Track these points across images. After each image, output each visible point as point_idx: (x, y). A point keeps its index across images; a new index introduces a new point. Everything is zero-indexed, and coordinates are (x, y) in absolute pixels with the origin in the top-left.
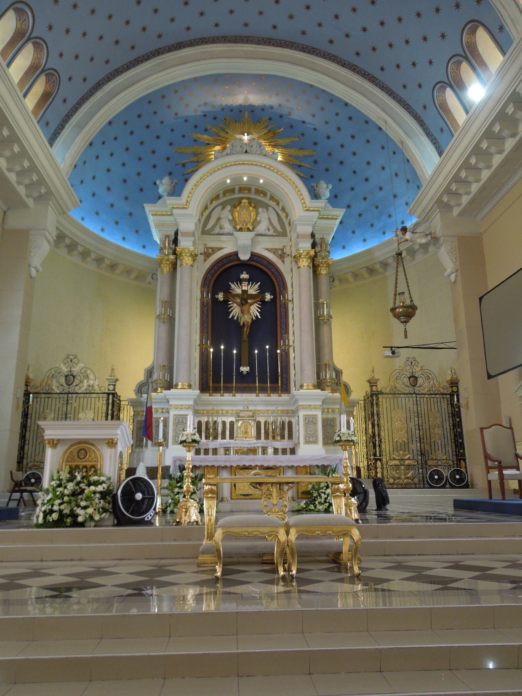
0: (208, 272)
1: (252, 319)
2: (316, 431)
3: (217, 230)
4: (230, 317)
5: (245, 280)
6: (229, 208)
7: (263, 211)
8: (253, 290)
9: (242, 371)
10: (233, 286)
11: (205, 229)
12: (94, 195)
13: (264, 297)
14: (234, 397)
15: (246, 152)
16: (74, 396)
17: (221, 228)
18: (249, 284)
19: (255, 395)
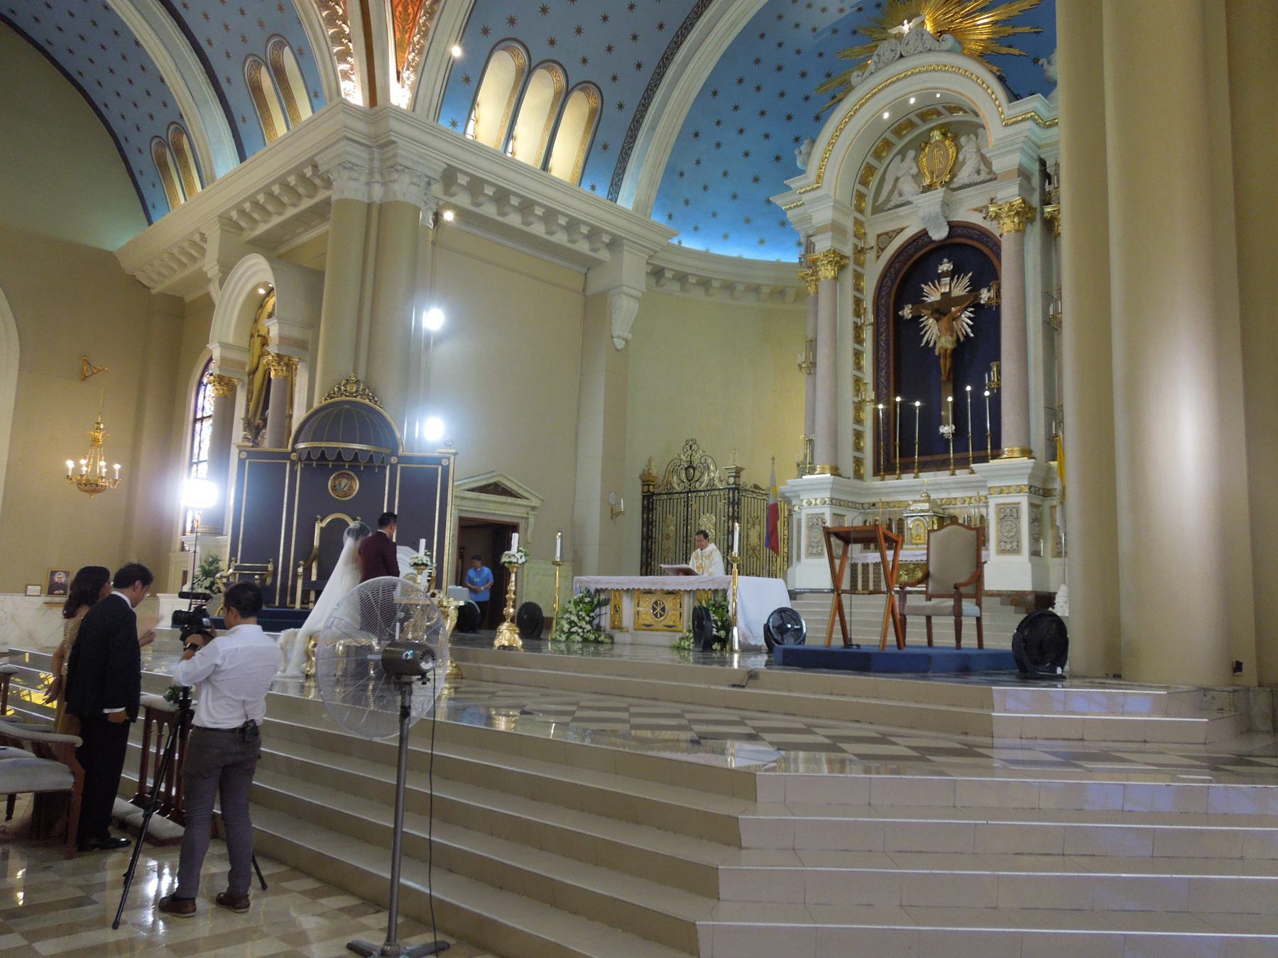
0: (884, 276)
1: (958, 338)
2: (1018, 531)
3: (896, 200)
4: (922, 345)
5: (945, 274)
6: (911, 154)
7: (968, 142)
8: (960, 289)
9: (943, 434)
10: (926, 288)
11: (877, 204)
12: (735, 197)
13: (977, 297)
14: (954, 477)
15: (902, 56)
16: (694, 494)
17: (901, 195)
18: (952, 280)
19: (948, 472)
